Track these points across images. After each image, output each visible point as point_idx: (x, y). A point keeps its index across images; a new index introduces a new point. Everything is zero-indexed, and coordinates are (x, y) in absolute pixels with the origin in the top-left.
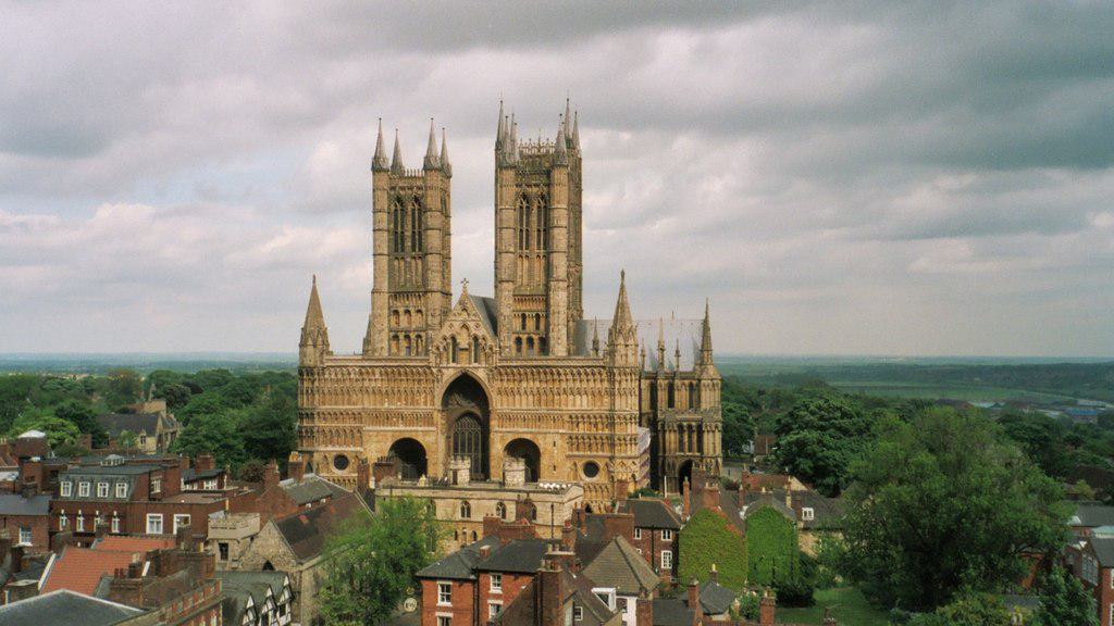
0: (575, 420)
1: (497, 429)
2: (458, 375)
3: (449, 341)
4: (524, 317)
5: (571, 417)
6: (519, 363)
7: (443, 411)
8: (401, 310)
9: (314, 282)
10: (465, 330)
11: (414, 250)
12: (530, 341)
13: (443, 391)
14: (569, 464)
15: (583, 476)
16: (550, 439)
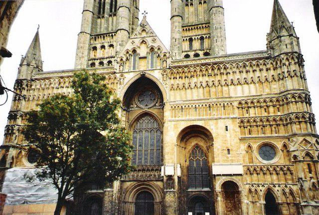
0: (244, 105)
1: (170, 118)
2: (139, 76)
3: (130, 53)
4: (191, 40)
5: (240, 103)
6: (189, 63)
7: (124, 110)
8: (98, 46)
9: (38, 28)
10: (143, 46)
11: (111, 11)
12: (197, 55)
13: (124, 90)
14: (244, 147)
15: (260, 159)
16: (222, 124)
